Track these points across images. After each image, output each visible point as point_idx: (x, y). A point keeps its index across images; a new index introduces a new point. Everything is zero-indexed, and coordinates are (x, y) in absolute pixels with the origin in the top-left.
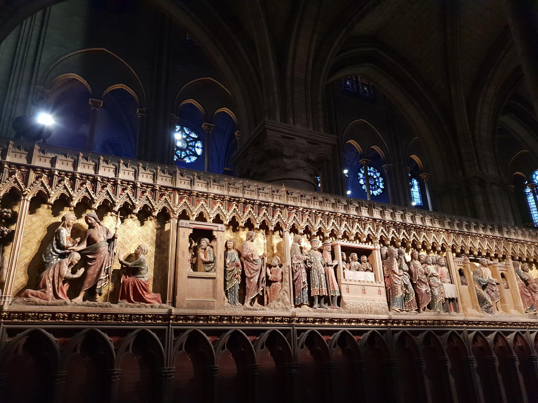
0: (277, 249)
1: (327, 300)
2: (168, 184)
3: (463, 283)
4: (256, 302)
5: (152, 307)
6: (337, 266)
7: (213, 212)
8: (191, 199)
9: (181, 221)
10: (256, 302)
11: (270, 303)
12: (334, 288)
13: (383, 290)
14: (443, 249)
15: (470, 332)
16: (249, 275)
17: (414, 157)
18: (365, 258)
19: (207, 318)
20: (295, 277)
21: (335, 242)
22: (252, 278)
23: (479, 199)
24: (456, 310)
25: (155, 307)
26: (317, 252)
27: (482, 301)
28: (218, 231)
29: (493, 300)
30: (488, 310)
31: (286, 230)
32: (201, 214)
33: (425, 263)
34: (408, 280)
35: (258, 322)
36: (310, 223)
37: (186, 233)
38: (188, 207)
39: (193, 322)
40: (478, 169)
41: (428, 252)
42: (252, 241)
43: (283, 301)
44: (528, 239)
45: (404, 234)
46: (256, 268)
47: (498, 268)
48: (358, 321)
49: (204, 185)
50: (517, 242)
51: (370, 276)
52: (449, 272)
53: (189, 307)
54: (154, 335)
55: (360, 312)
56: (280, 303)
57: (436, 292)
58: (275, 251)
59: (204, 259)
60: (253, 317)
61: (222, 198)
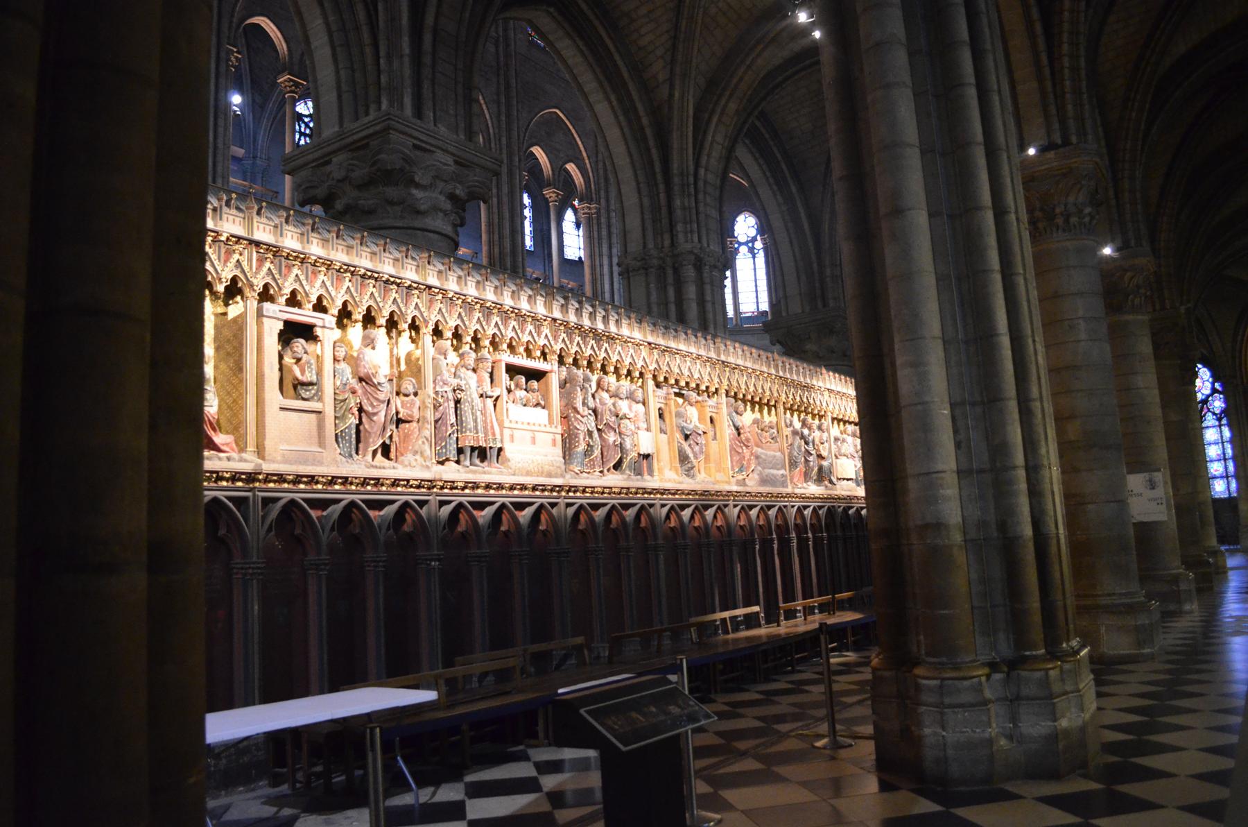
0: (406, 363)
1: (482, 454)
2: (240, 231)
3: (662, 431)
4: (379, 455)
5: (229, 459)
6: (498, 398)
7: (314, 290)
8: (277, 261)
9: (267, 306)
10: (379, 455)
11: (400, 459)
12: (494, 434)
13: (559, 438)
14: (641, 374)
15: (663, 506)
16: (370, 409)
17: (538, 151)
18: (535, 384)
19: (312, 479)
20: (438, 415)
21: (498, 357)
22: (375, 414)
23: (691, 291)
24: (651, 473)
25: (234, 460)
26: (470, 373)
27: (683, 458)
28: (324, 327)
29: (696, 457)
30: (689, 472)
31: (426, 332)
32: (294, 293)
33: (615, 395)
34: (593, 424)
35: (384, 488)
36: (463, 321)
37: (273, 328)
38: (274, 279)
39: (291, 486)
40: (696, 239)
41: (619, 377)
42: (373, 348)
43: (422, 454)
44: (749, 364)
45: (592, 347)
46: (382, 396)
47: (708, 409)
48: (524, 487)
49: (295, 236)
50: (736, 368)
51: (541, 414)
52: (647, 413)
53: (286, 461)
54: (231, 505)
55: (528, 473)
56: (418, 457)
57: (628, 444)
58: (403, 367)
59: (300, 377)
60: (378, 479)
61: (329, 265)
